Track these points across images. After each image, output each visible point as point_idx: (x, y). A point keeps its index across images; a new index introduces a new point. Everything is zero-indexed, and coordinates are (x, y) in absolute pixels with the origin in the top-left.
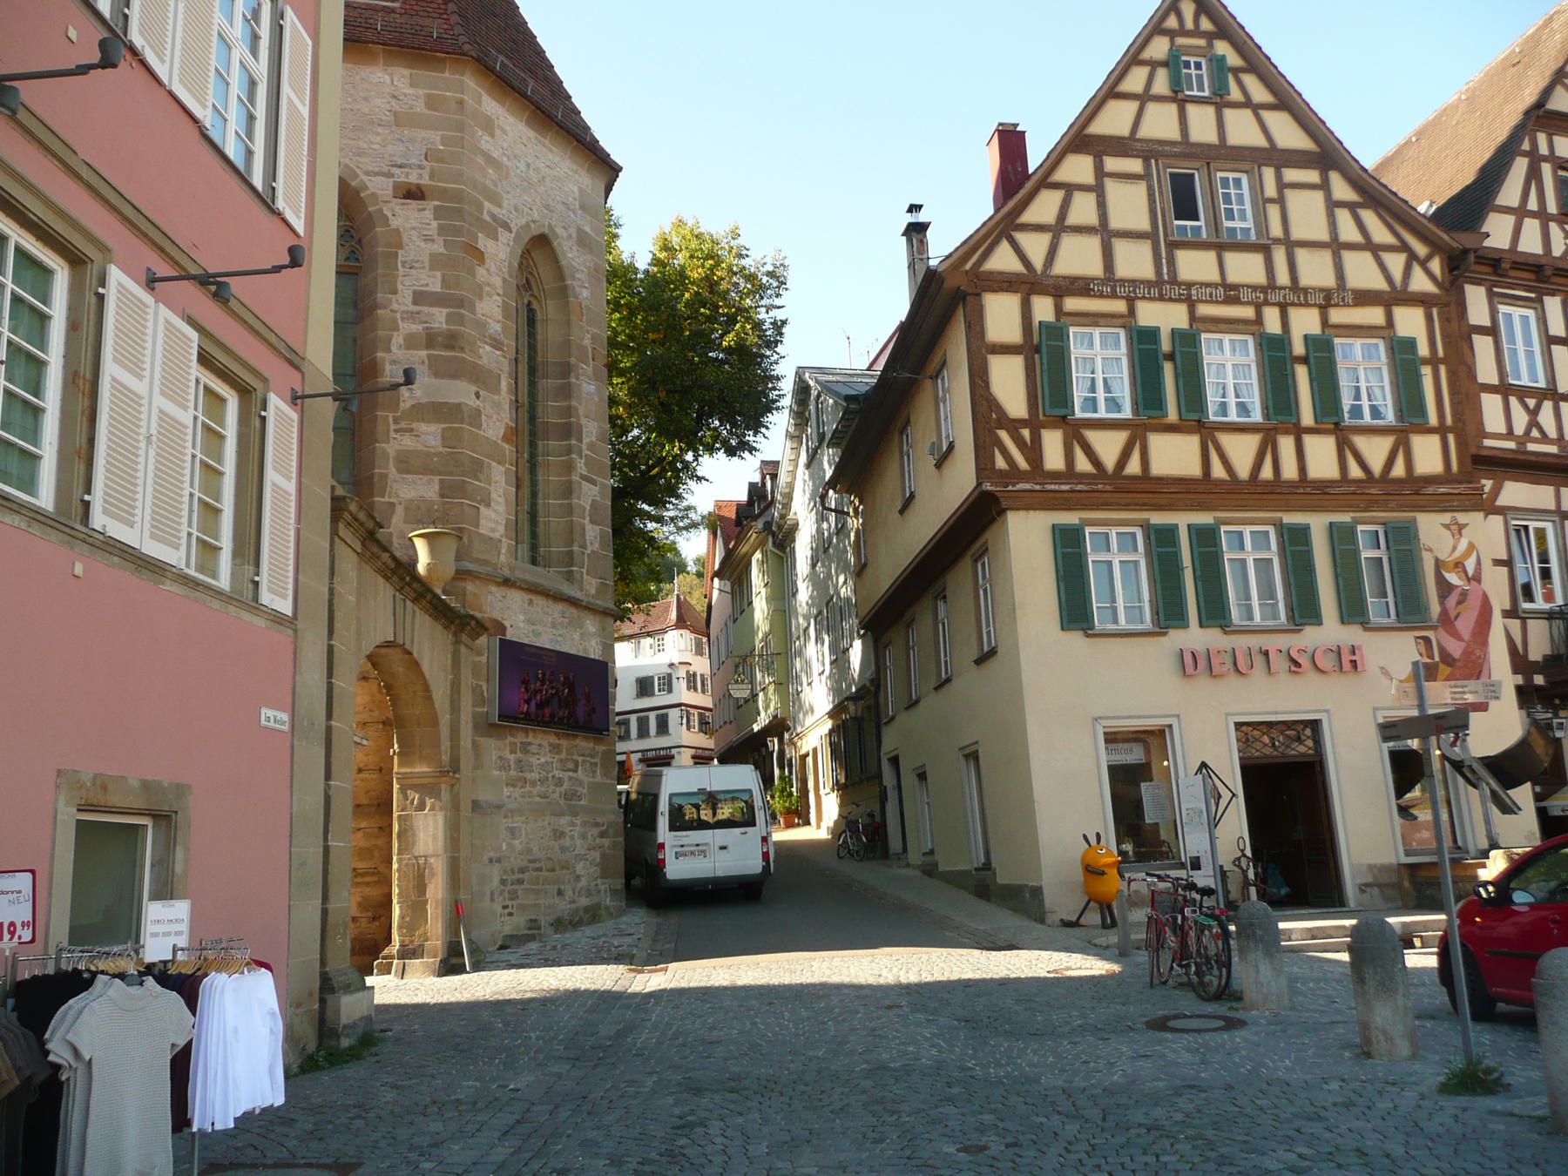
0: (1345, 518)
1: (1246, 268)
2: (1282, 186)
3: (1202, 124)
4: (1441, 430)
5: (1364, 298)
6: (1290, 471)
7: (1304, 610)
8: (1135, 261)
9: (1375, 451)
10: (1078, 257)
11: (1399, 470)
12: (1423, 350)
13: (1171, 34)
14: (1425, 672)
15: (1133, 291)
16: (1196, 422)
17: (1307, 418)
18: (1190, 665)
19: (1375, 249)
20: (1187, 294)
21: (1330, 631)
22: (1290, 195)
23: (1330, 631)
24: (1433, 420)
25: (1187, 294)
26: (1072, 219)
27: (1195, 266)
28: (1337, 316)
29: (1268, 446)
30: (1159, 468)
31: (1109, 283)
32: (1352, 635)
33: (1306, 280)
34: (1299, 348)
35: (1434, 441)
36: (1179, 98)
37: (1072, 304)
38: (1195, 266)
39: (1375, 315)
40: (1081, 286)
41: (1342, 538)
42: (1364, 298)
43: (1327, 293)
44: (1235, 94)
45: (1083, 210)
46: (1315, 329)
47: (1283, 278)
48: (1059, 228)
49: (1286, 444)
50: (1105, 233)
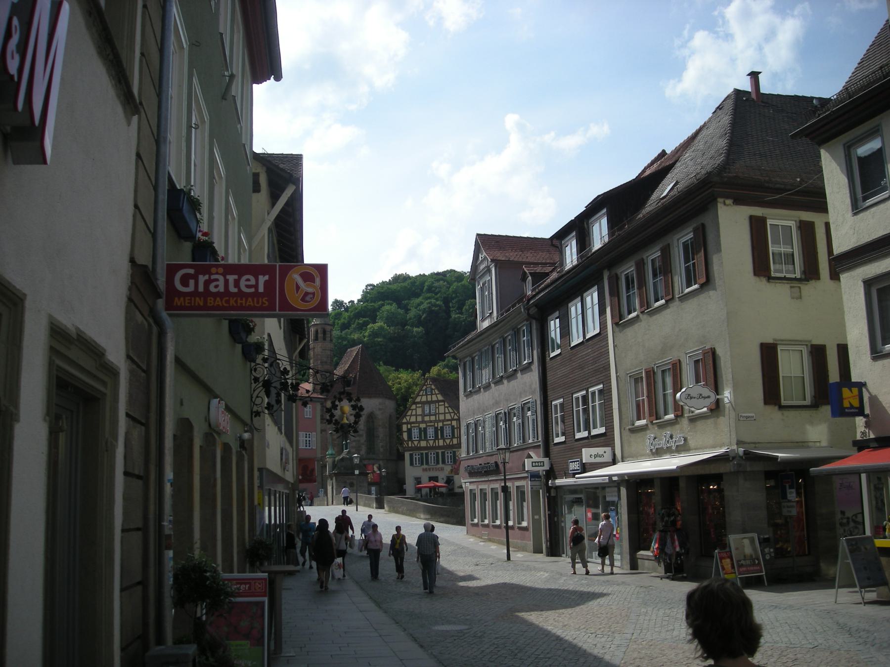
0: (443, 450)
1: (433, 418)
2: (439, 405)
3: (429, 398)
4: (457, 438)
5: (448, 420)
6: (437, 445)
7: (438, 463)
8: (419, 419)
9: (448, 441)
10: (413, 419)
11: (451, 443)
12: (456, 427)
13: (426, 385)
14: (452, 470)
15: (419, 423)
16: (426, 439)
17: (440, 438)
18: (425, 470)
19: (450, 413)
20: (425, 422)
21: (441, 465)
22: (440, 407)
23: (441, 465)
24: (456, 436)
25: (425, 422)
26: (413, 414)
27: (427, 418)
28: (445, 423)
29: (435, 441)
30: (422, 445)
31: (416, 422)
32: (443, 466)
33: (440, 419)
34: (439, 428)
35: (456, 439)
36: (427, 395)
37: (412, 425)
38: (427, 418)
39: (449, 422)
40: (413, 423)
41: (443, 453)
42: (448, 420)
43: (443, 420)
44: (434, 393)
45: (414, 411)
46: (442, 425)
47: (437, 419)
48: (411, 415)
49: (437, 441)
50: (416, 415)
